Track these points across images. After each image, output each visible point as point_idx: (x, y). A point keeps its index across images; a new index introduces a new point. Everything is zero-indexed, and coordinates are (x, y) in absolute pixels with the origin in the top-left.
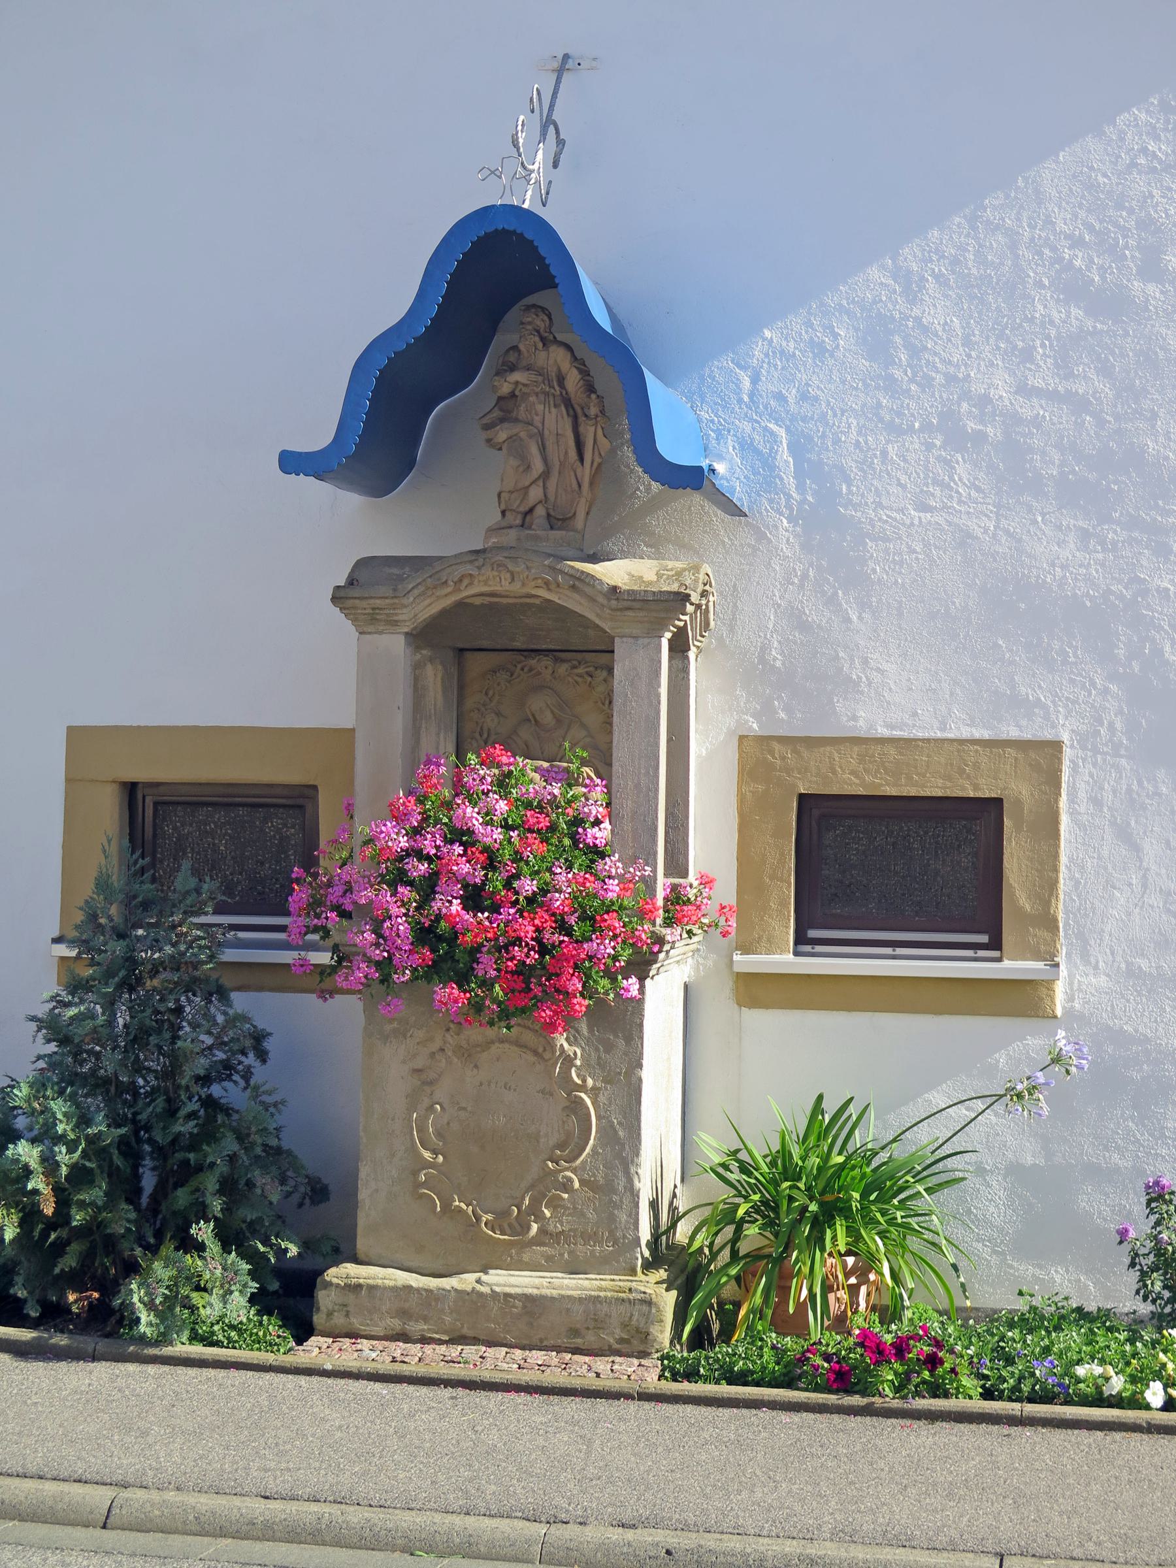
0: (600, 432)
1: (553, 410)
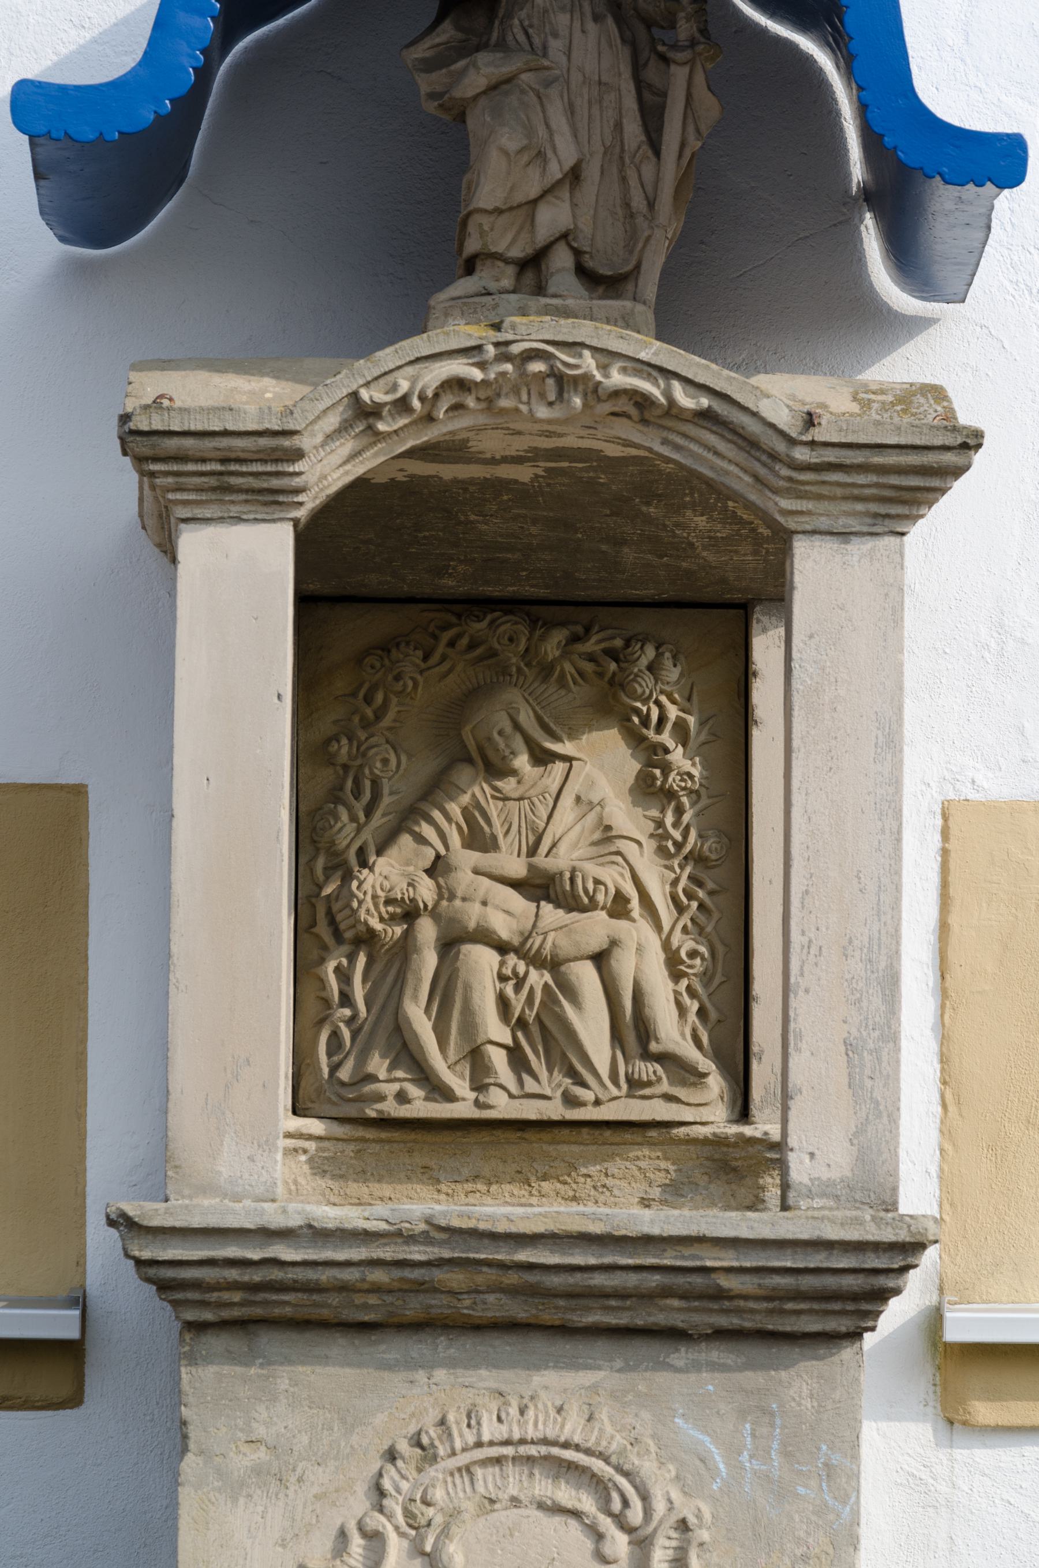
0: (700, 78)
1: (591, 26)
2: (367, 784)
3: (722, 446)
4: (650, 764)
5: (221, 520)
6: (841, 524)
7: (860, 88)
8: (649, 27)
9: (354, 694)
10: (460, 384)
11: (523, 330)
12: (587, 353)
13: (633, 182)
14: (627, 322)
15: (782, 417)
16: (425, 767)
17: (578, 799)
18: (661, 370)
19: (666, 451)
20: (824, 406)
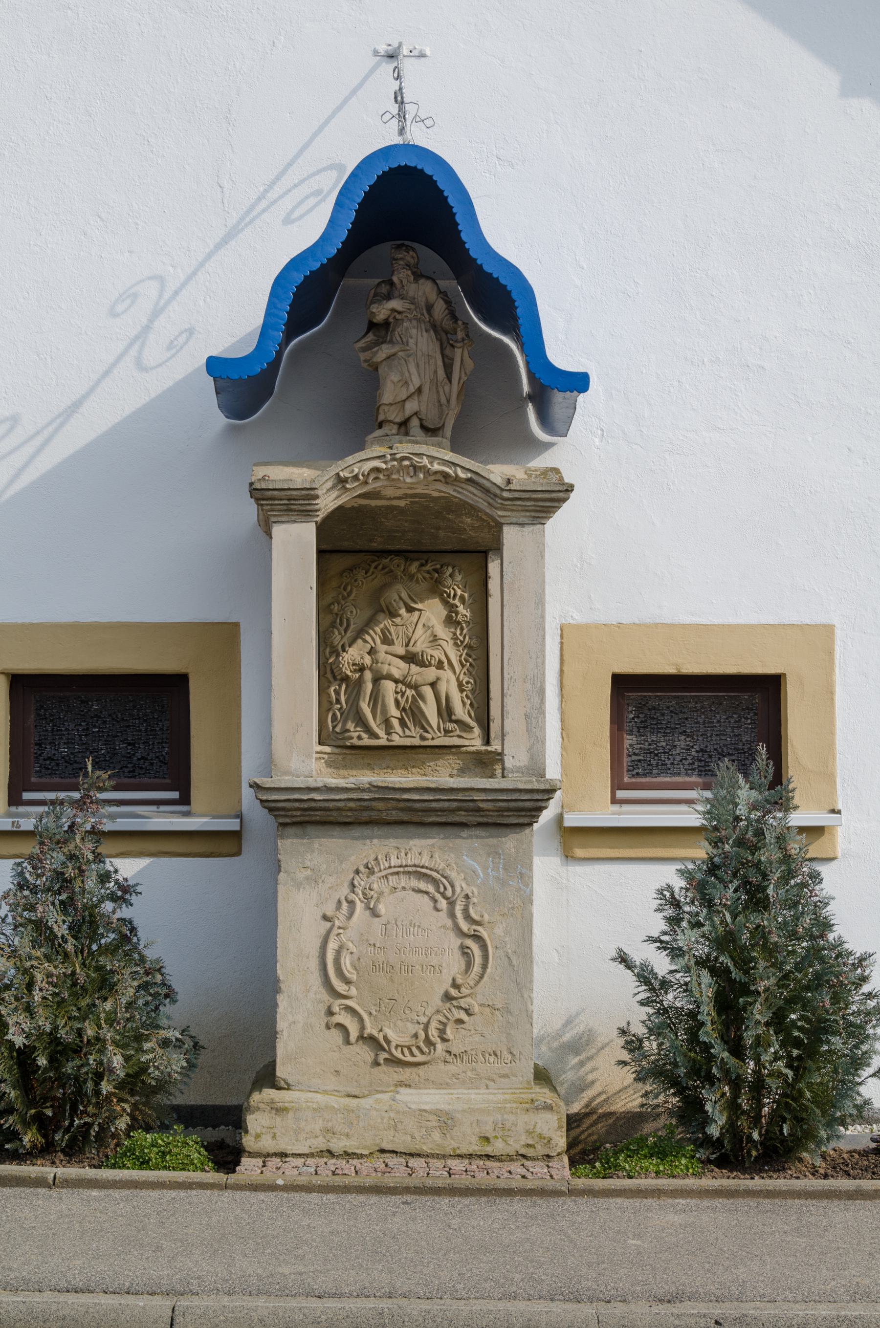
0: (466, 353)
1: (425, 334)
2: (345, 620)
3: (476, 492)
4: (451, 612)
5: (288, 522)
6: (521, 520)
7: (527, 356)
8: (446, 334)
9: (339, 587)
10: (377, 470)
11: (400, 449)
12: (425, 457)
13: (441, 393)
14: (440, 445)
15: (498, 481)
16: (367, 613)
17: (424, 625)
18: (453, 463)
19: (455, 494)
20: (514, 476)
